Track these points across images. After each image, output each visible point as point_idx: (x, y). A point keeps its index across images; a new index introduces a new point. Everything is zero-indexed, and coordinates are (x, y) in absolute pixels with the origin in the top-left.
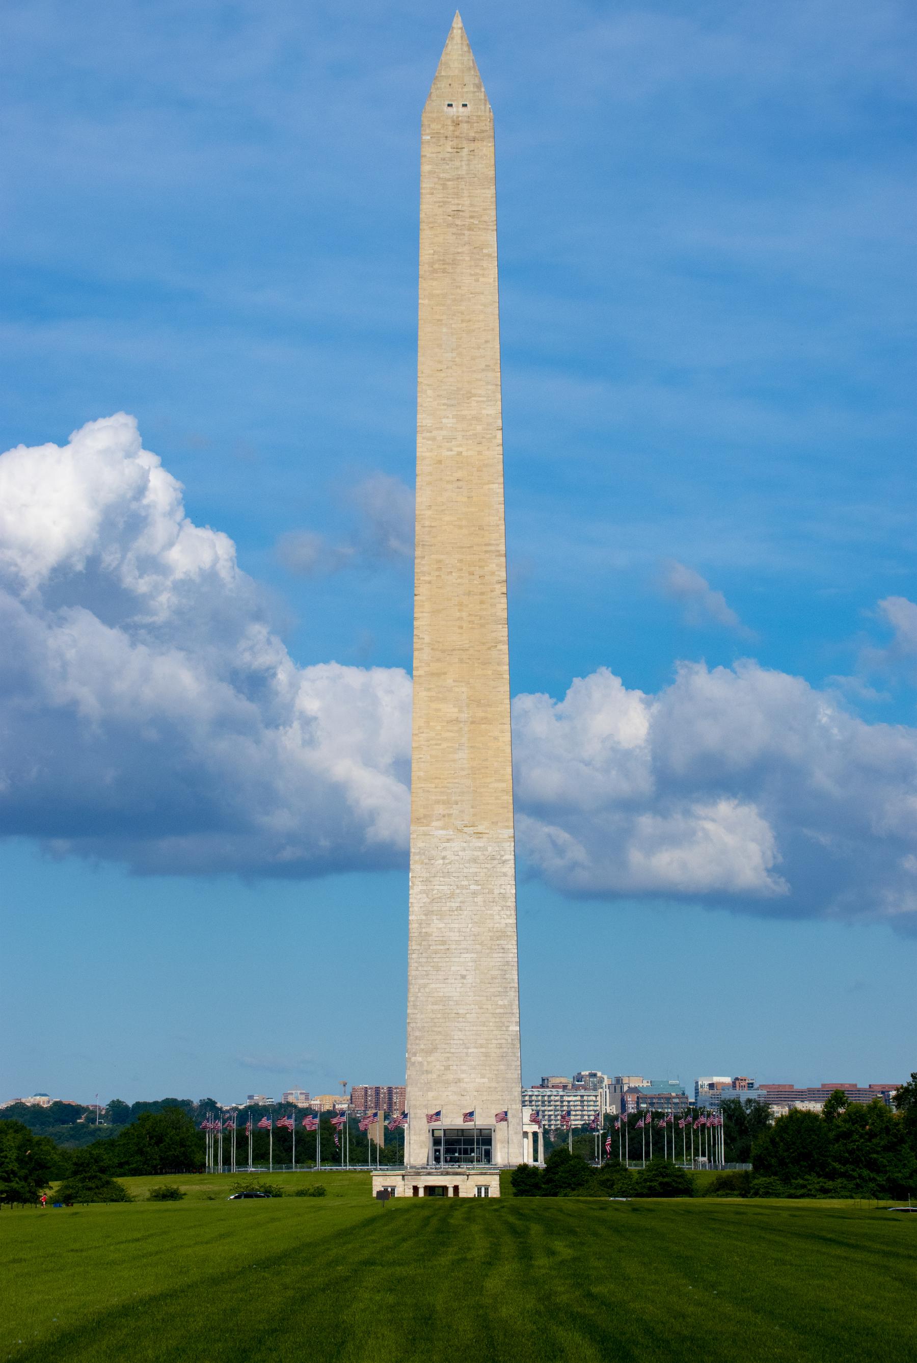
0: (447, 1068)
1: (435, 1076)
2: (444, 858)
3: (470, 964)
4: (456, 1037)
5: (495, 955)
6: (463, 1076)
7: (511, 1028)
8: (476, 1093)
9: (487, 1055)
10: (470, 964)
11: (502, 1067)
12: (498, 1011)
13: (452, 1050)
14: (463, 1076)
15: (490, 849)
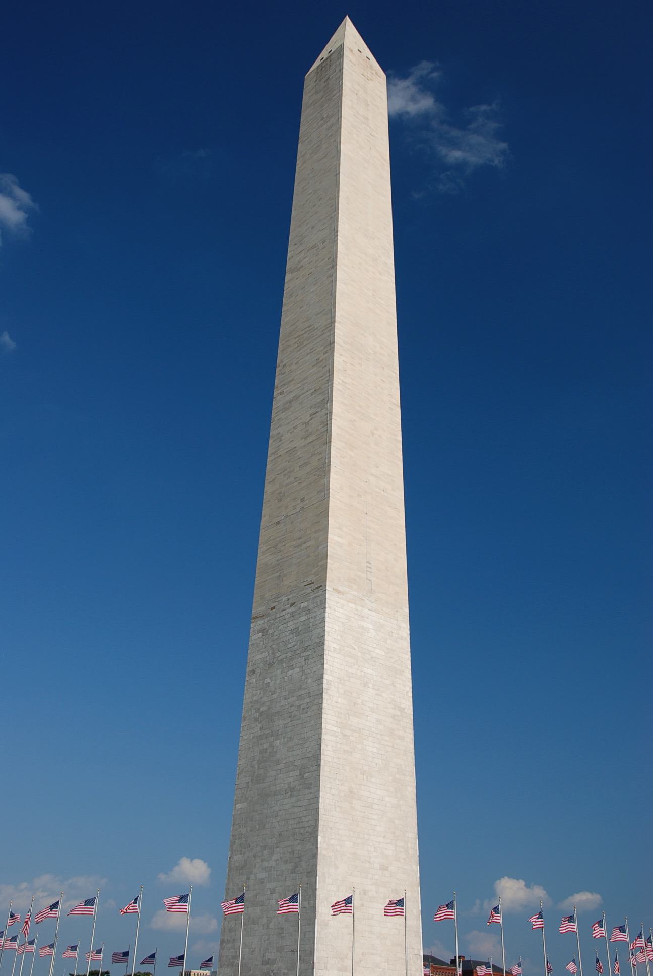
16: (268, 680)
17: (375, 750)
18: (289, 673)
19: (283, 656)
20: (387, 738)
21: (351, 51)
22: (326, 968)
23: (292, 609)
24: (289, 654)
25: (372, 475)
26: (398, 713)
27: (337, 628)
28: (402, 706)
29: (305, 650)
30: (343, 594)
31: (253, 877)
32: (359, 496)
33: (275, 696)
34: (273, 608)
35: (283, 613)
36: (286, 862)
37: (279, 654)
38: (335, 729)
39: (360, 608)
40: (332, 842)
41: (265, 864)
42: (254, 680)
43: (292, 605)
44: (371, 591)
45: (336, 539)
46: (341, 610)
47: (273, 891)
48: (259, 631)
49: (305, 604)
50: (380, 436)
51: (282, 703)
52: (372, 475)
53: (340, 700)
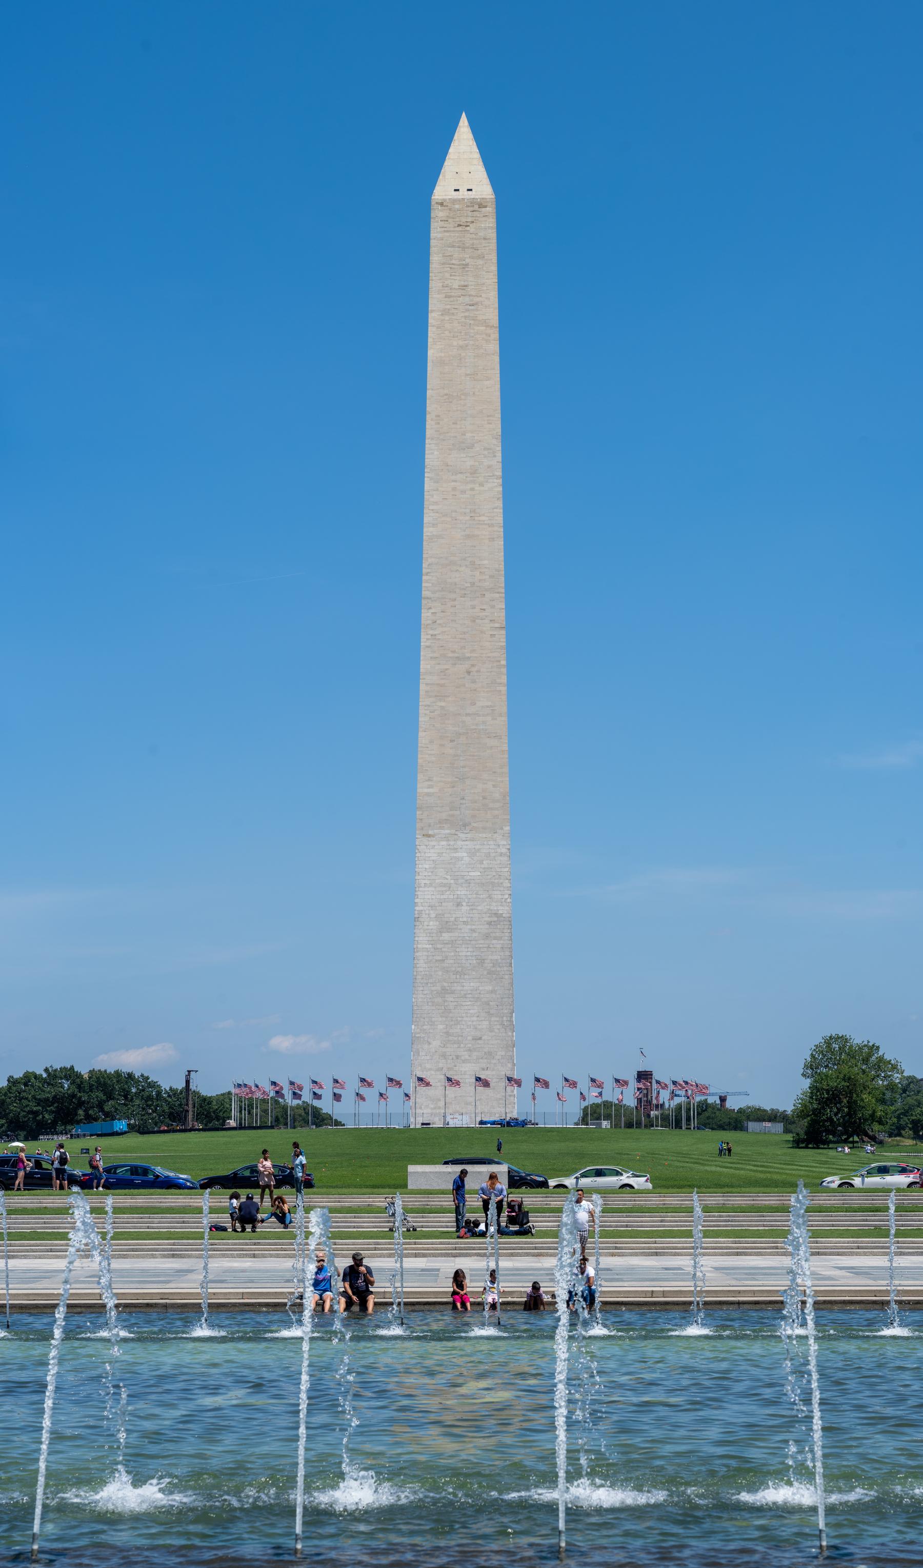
17: (469, 954)
20: (482, 942)
21: (442, 204)
22: (421, 1108)
25: (467, 715)
26: (496, 919)
27: (427, 866)
28: (500, 912)
30: (433, 836)
32: (451, 741)
38: (427, 946)
39: (452, 843)
40: (425, 1027)
44: (465, 825)
45: (426, 790)
46: (432, 851)
50: (478, 671)
52: (467, 715)
53: (431, 923)
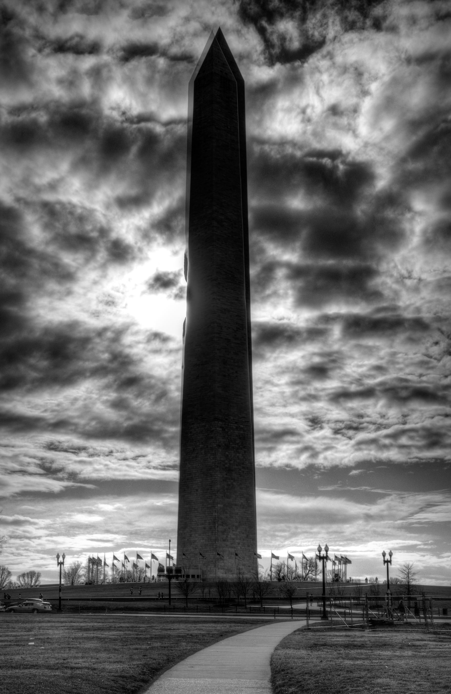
0: (191, 535)
1: (186, 540)
2: (191, 433)
3: (199, 484)
4: (194, 520)
5: (208, 478)
6: (196, 539)
7: (214, 514)
8: (200, 547)
9: (204, 528)
10: (199, 484)
11: (210, 534)
12: (209, 506)
13: (193, 527)
14: (196, 539)
15: (207, 426)
16: (227, 453)
18: (238, 455)
19: (234, 445)
23: (236, 425)
24: (237, 446)
29: (244, 447)
31: (229, 536)
33: (232, 462)
34: (227, 419)
35: (232, 424)
36: (243, 533)
37: (231, 443)
41: (234, 532)
42: (220, 450)
43: (236, 423)
47: (239, 544)
48: (221, 427)
49: (242, 426)
51: (236, 467)
